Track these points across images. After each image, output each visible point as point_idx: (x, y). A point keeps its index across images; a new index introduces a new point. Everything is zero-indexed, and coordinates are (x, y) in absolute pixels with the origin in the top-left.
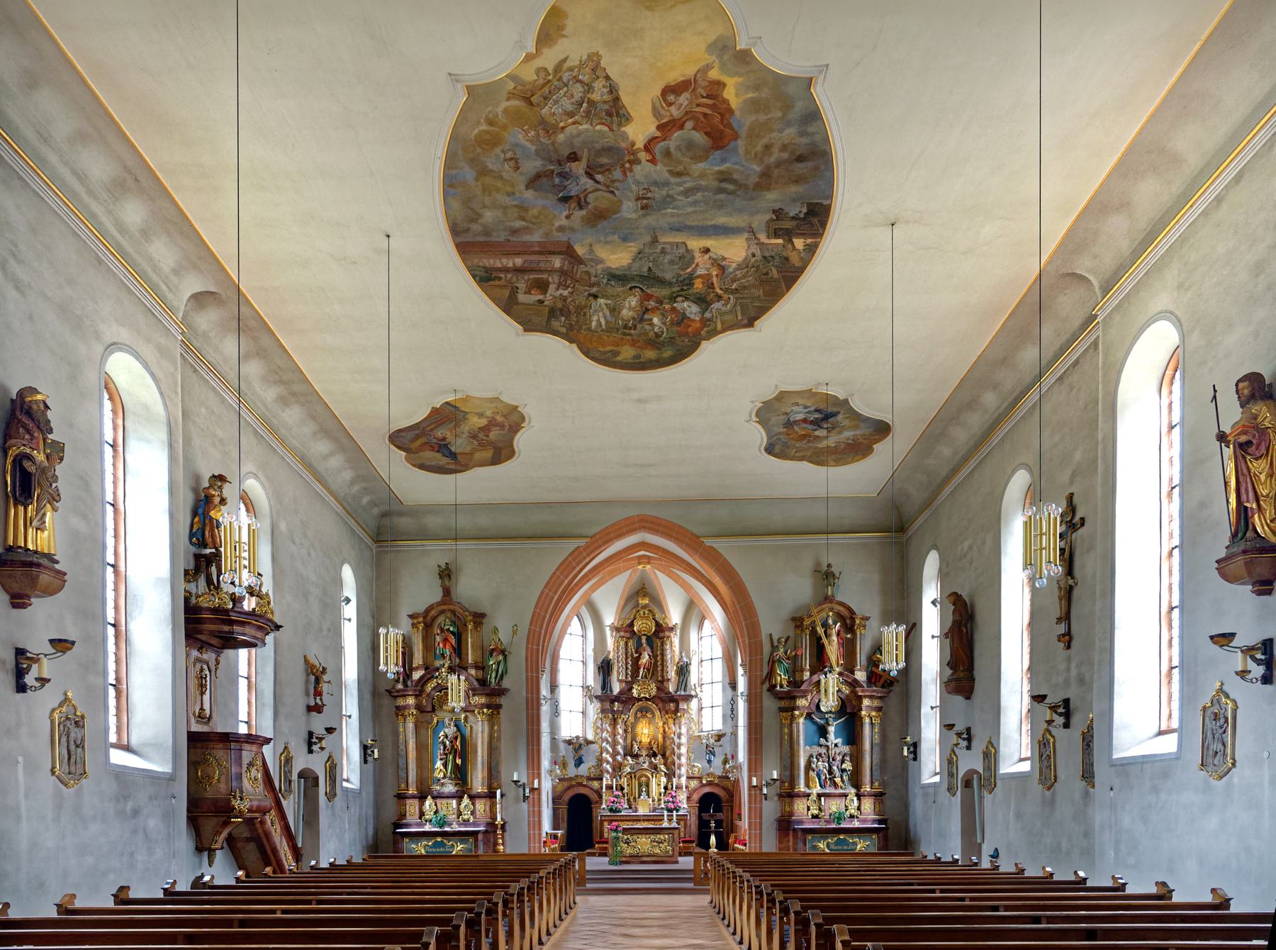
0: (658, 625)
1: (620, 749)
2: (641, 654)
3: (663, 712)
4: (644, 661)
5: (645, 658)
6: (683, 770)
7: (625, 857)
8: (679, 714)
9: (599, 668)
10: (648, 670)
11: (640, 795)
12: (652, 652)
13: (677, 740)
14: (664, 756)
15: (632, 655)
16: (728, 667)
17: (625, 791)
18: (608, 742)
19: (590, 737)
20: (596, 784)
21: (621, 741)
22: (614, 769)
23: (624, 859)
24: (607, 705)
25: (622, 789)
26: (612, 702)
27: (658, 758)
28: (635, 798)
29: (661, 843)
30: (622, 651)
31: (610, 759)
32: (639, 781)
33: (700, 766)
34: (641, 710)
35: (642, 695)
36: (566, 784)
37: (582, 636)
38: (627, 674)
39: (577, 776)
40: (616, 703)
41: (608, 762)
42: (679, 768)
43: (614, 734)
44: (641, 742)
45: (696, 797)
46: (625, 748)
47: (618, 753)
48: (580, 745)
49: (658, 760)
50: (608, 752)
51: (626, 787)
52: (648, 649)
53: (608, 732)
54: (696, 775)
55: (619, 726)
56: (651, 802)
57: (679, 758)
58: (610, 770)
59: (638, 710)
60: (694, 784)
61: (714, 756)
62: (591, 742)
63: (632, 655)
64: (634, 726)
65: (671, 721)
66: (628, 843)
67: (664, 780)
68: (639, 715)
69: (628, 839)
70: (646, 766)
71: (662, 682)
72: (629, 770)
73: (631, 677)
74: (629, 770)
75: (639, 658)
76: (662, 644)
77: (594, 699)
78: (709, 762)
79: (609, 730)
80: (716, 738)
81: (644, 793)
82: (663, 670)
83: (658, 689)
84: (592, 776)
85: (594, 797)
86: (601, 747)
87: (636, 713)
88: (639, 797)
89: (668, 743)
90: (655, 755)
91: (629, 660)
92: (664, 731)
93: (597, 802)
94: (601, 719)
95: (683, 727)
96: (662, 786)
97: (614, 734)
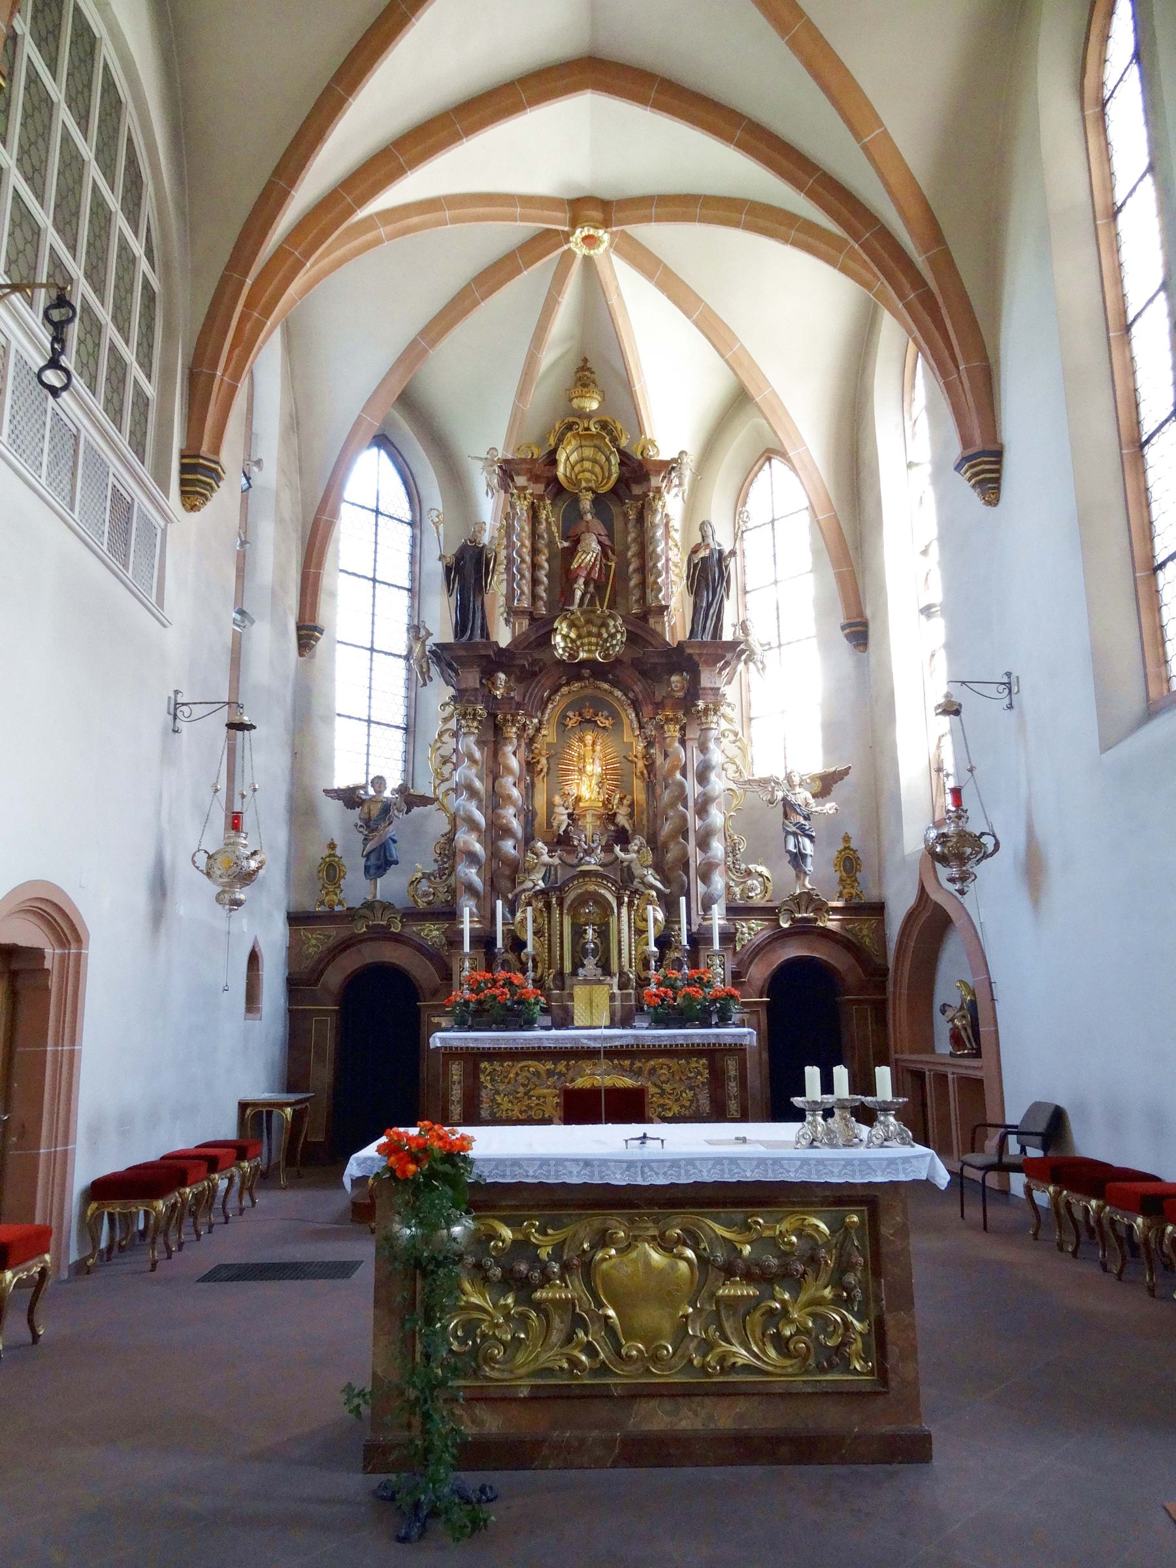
0: (625, 458)
1: (510, 817)
2: (577, 541)
3: (647, 710)
4: (589, 558)
5: (589, 553)
6: (719, 881)
7: (501, 1399)
8: (701, 704)
9: (448, 570)
10: (600, 587)
11: (577, 964)
12: (610, 536)
13: (693, 789)
14: (652, 841)
15: (551, 543)
16: (840, 577)
17: (530, 949)
18: (473, 793)
19: (424, 787)
20: (432, 932)
21: (515, 793)
22: (494, 887)
23: (492, 1423)
24: (472, 678)
25: (517, 944)
26: (488, 674)
27: (634, 846)
28: (561, 973)
29: (796, 1284)
30: (522, 527)
31: (478, 848)
32: (574, 917)
33: (766, 872)
34: (577, 705)
35: (582, 655)
36: (334, 933)
37: (412, 524)
38: (535, 597)
39: (369, 906)
40: (502, 676)
41: (472, 857)
42: (705, 877)
43: (494, 771)
44: (578, 799)
45: (759, 973)
46: (528, 817)
47: (507, 832)
48: (386, 808)
49: (635, 855)
50: (473, 825)
51: (529, 938)
52: (600, 528)
53: (473, 761)
54: (757, 898)
55: (509, 749)
56: (616, 990)
57: (704, 843)
58: (478, 882)
59: (568, 707)
60: (752, 930)
61: (811, 838)
62: (424, 801)
63: (551, 543)
64: (556, 755)
65: (673, 731)
66: (523, 1286)
67: (655, 913)
68: (573, 720)
69: (523, 1247)
70: (592, 864)
71: (644, 617)
72: (541, 884)
73: (550, 605)
74: (541, 884)
75: (571, 553)
76: (641, 518)
77: (435, 671)
78: (798, 858)
79: (477, 755)
80: (817, 786)
81: (590, 962)
82: (643, 584)
83: (633, 639)
84: (421, 904)
85: (421, 971)
86: (453, 820)
87: (564, 716)
88: (574, 973)
89: (666, 796)
90: (622, 838)
91: (542, 559)
92: (650, 767)
93: (435, 993)
94: (455, 735)
95: (712, 745)
96: (652, 935)
97: (494, 771)
